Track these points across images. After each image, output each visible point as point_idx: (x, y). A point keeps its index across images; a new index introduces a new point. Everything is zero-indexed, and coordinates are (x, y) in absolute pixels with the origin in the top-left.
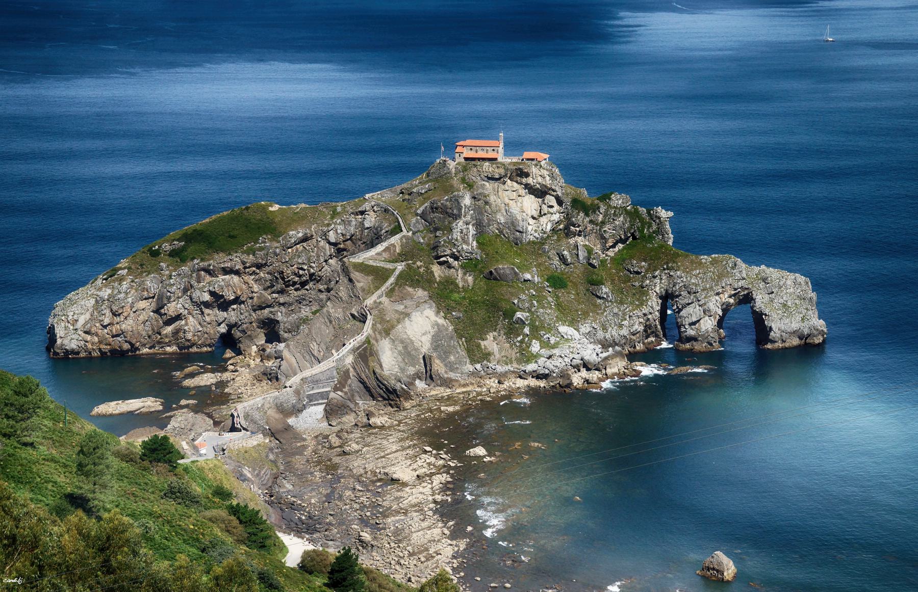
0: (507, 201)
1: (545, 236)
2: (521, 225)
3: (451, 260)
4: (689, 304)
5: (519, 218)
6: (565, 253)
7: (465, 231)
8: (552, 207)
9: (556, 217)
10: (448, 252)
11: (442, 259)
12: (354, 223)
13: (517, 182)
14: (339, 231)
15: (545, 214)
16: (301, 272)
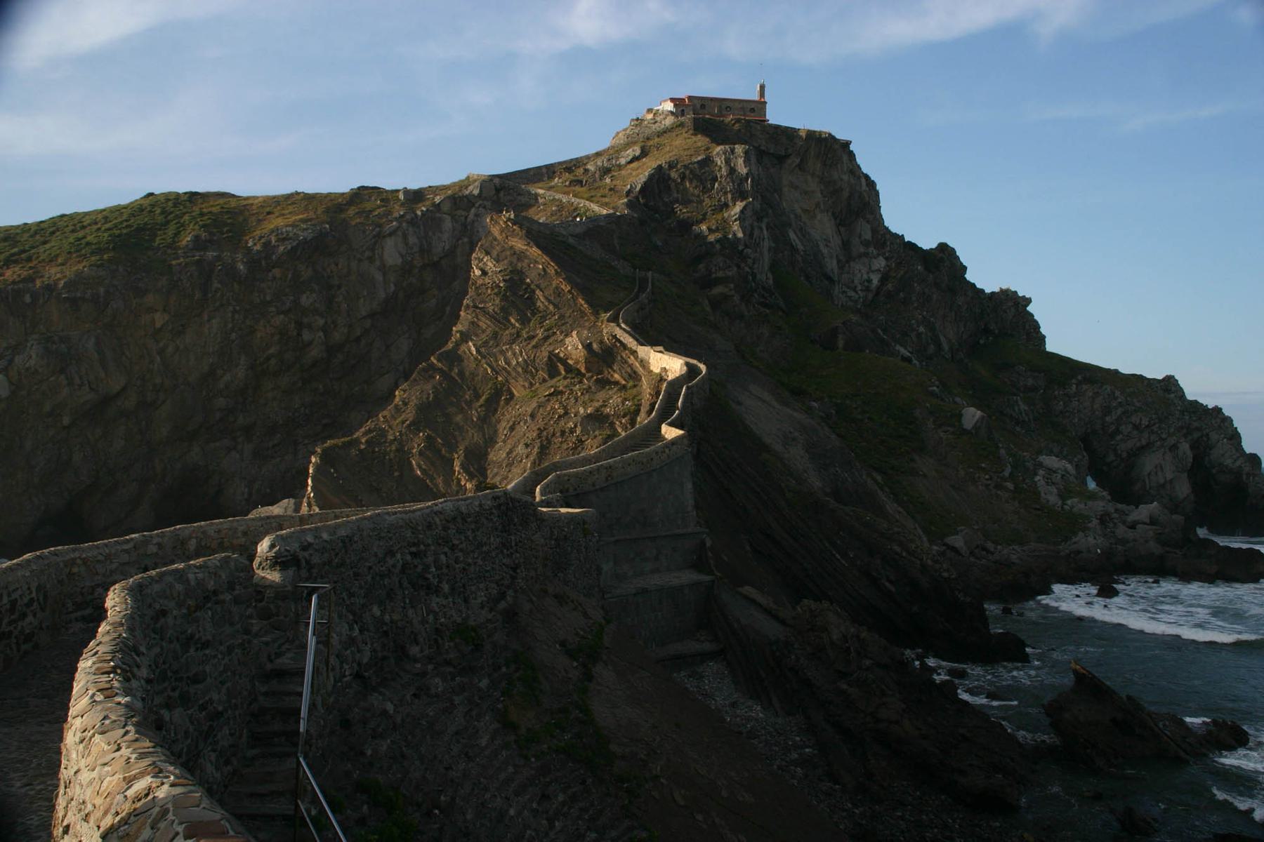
0: (799, 211)
1: (870, 296)
2: (831, 265)
3: (737, 298)
4: (1143, 447)
5: (825, 251)
6: (922, 329)
7: (756, 232)
8: (866, 244)
9: (880, 263)
10: (732, 272)
11: (718, 290)
12: (448, 224)
13: (813, 175)
14: (412, 240)
15: (860, 256)
16: (306, 336)
